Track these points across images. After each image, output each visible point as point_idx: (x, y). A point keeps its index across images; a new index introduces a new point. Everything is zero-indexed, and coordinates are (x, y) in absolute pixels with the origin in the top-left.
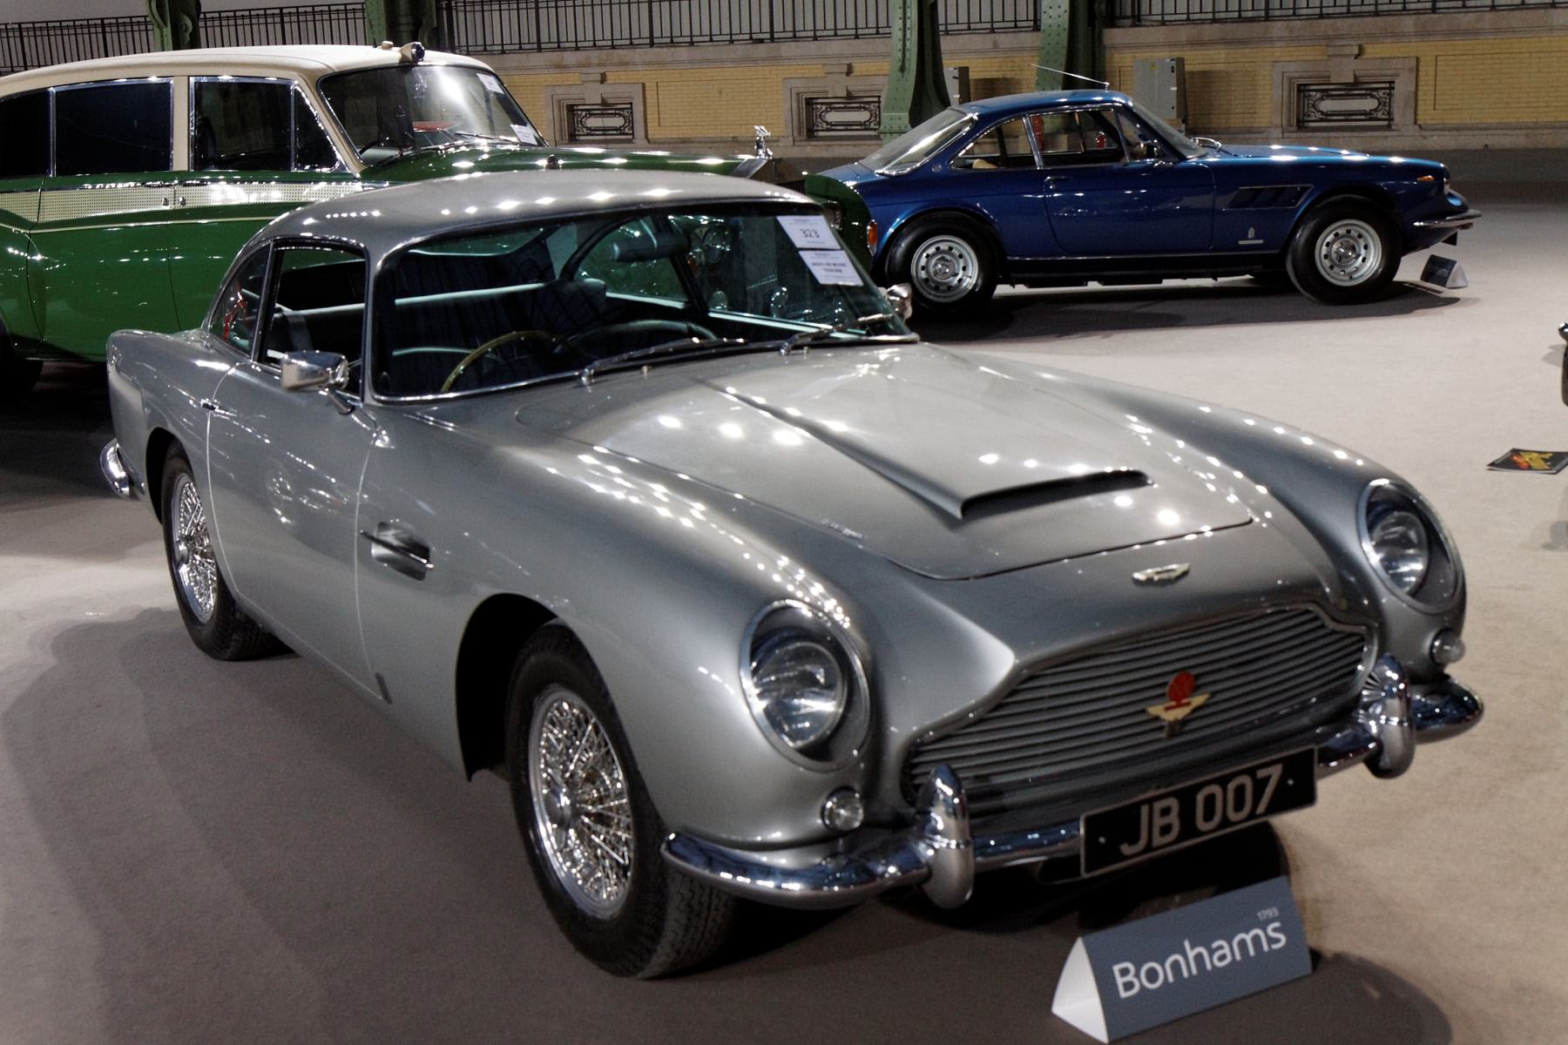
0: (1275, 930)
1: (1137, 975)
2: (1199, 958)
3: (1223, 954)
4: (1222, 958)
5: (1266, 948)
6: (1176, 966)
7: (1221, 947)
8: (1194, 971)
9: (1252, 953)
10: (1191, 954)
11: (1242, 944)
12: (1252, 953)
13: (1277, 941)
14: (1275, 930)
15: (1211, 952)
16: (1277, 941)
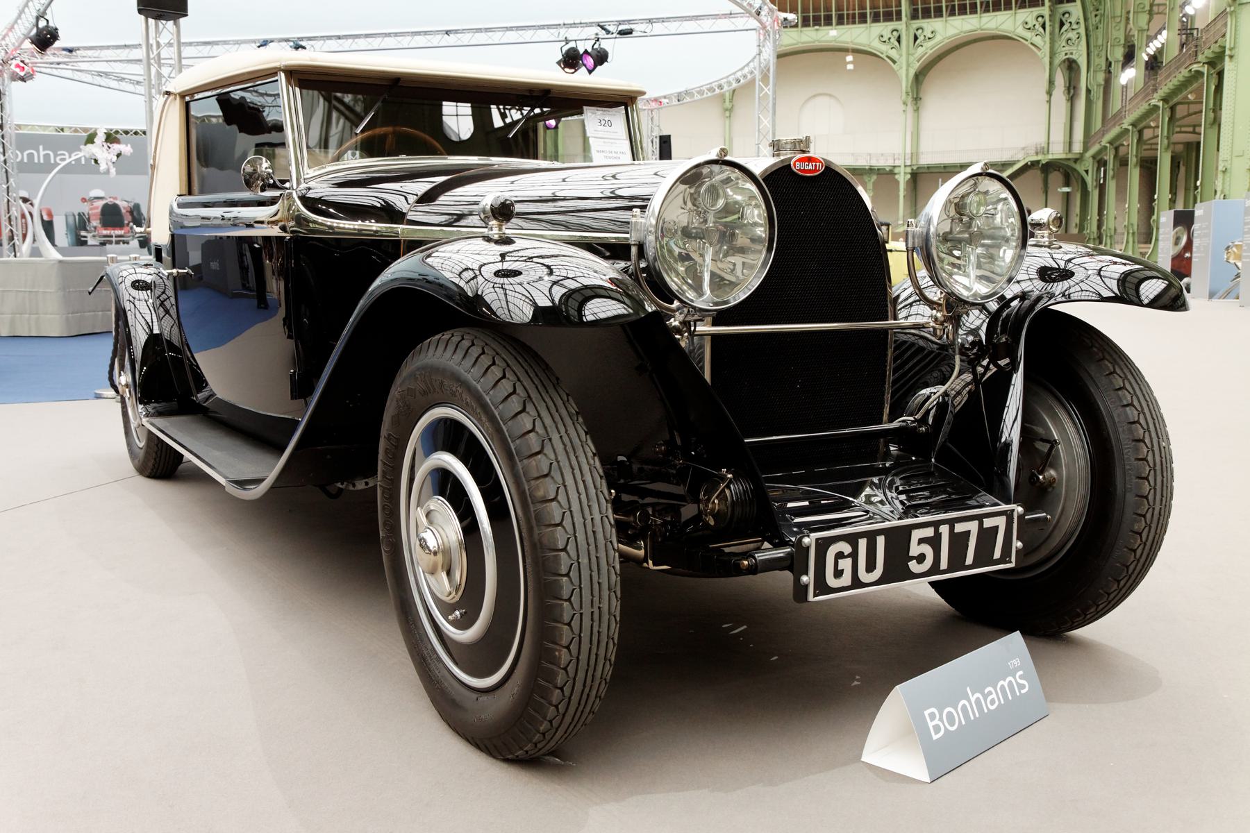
0: (1021, 677)
1: (941, 719)
3: (993, 699)
4: (992, 702)
6: (964, 708)
7: (990, 693)
10: (973, 700)
11: (1003, 687)
13: (1024, 687)
14: (1021, 677)
15: (985, 697)
16: (1024, 687)
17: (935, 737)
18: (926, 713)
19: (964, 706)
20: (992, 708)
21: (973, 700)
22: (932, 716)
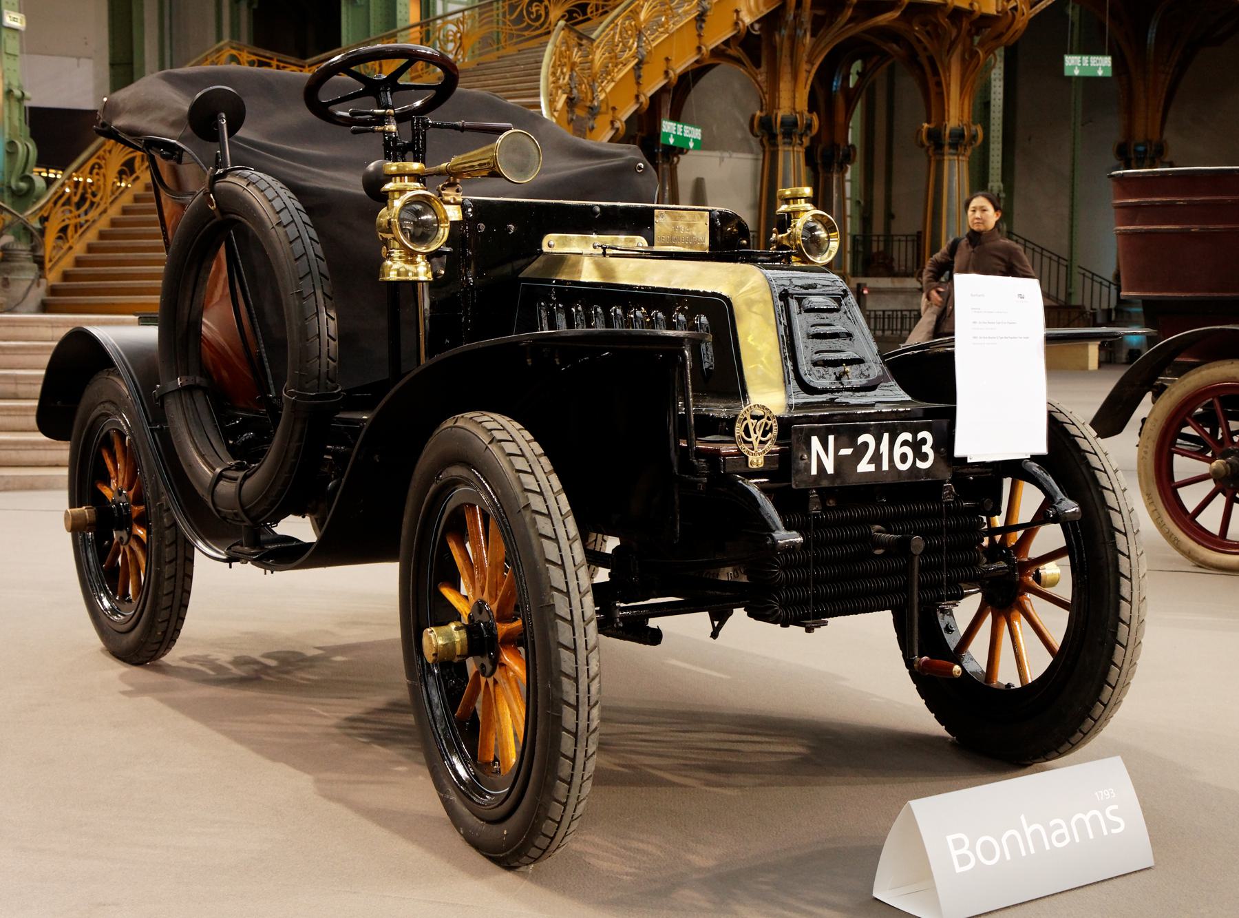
0: (1113, 813)
1: (972, 848)
2: (1036, 834)
4: (1061, 838)
5: (1105, 833)
6: (1012, 840)
7: (1059, 826)
8: (1033, 851)
9: (1091, 837)
10: (1028, 831)
11: (1080, 823)
12: (1091, 837)
13: (1118, 825)
14: (1113, 813)
15: (1049, 831)
16: (1118, 825)
17: (959, 870)
18: (950, 838)
19: (1012, 837)
21: (1028, 831)
22: (959, 844)
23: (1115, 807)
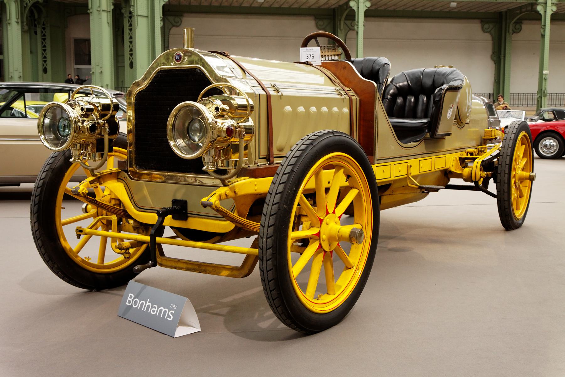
0: (171, 313)
1: (133, 300)
3: (155, 310)
4: (154, 311)
6: (142, 304)
7: (155, 308)
10: (147, 304)
11: (161, 310)
13: (170, 317)
14: (171, 313)
15: (152, 307)
16: (170, 317)
18: (130, 294)
19: (143, 303)
20: (152, 313)
21: (147, 304)
23: (173, 312)
